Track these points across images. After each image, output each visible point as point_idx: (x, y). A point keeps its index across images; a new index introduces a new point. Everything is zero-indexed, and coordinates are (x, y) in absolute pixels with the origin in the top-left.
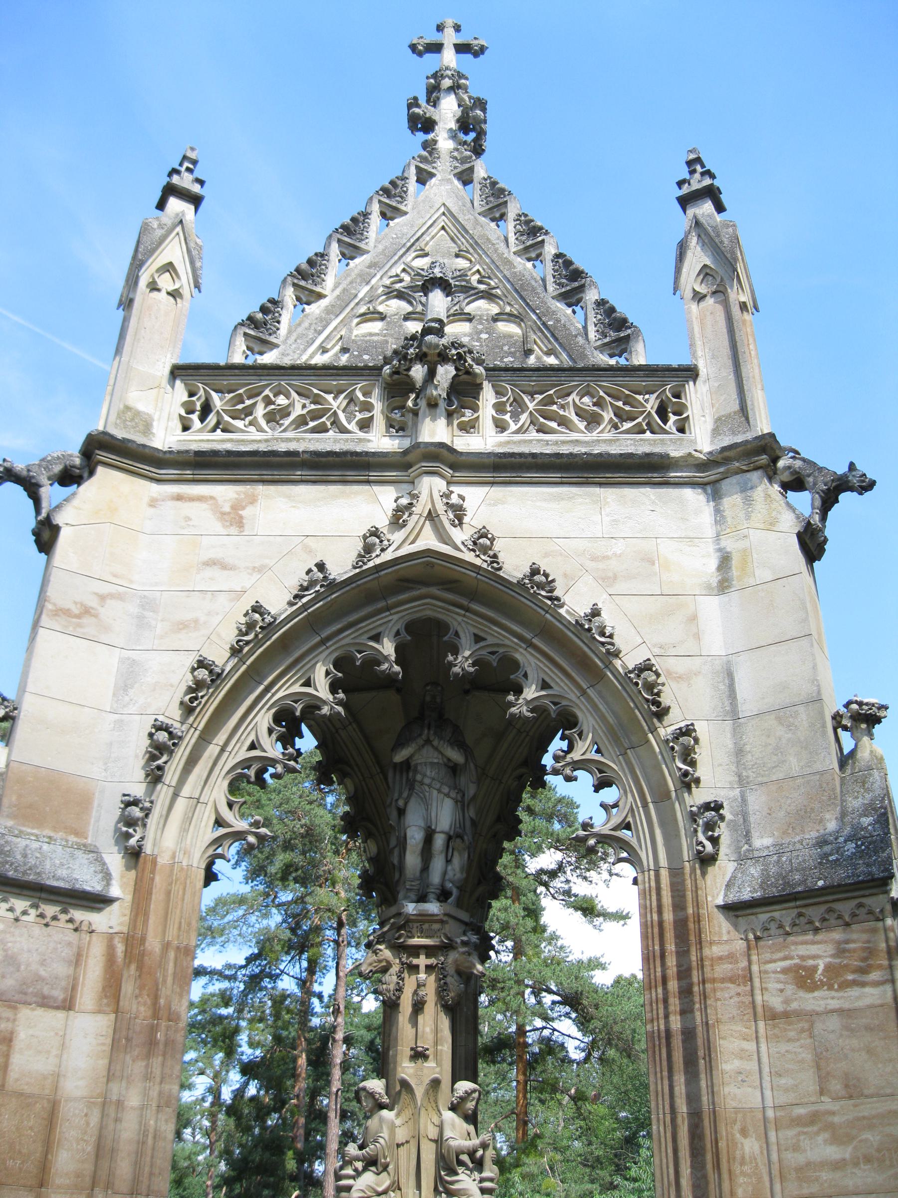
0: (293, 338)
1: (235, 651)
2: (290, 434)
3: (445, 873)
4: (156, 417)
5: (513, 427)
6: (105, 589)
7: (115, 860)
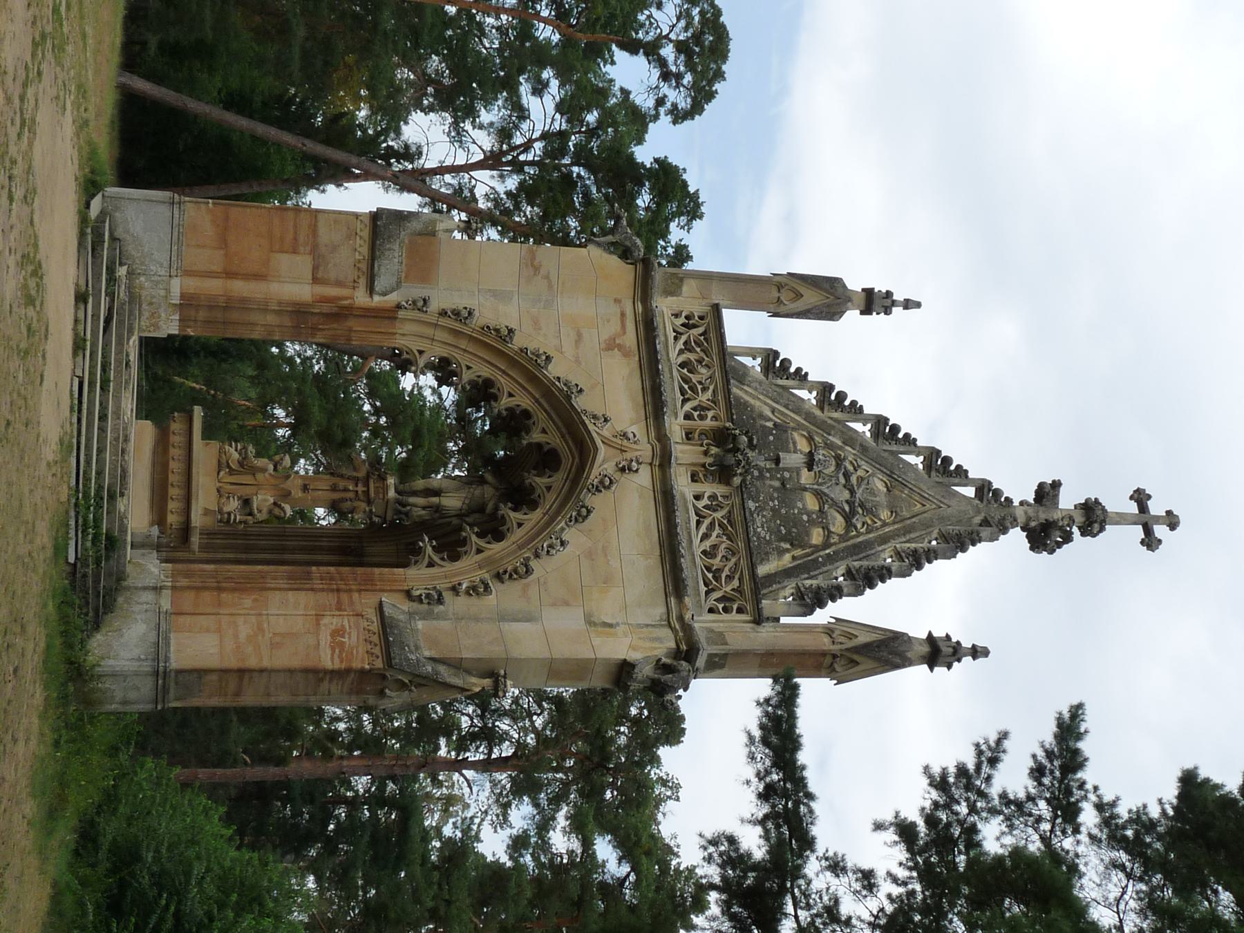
0: (777, 389)
1: (521, 350)
2: (675, 373)
3: (416, 506)
4: (680, 298)
5: (700, 505)
7: (393, 298)
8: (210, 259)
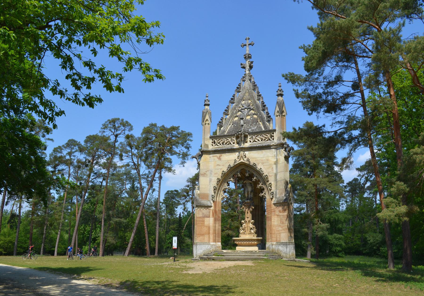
1: (221, 177)
5: (252, 141)
6: (207, 170)
7: (212, 202)
8: (206, 238)
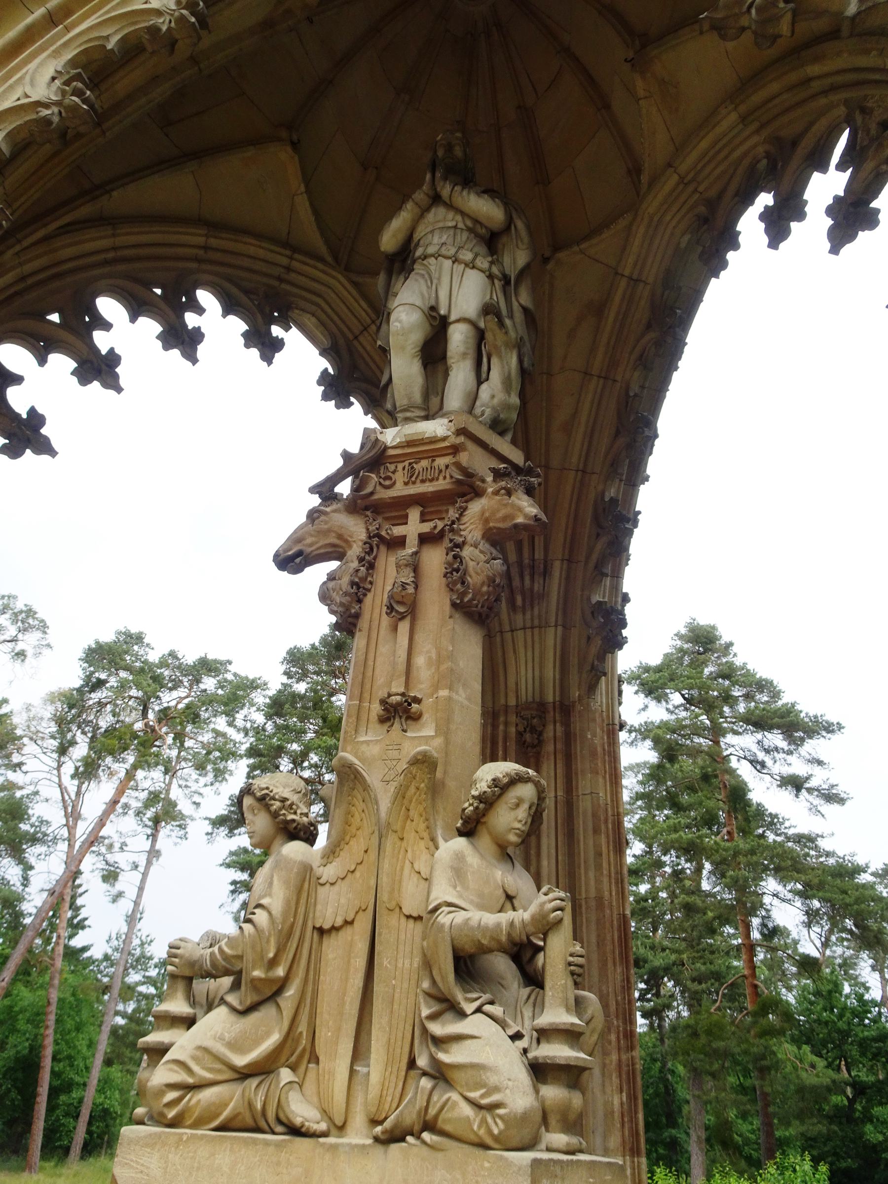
3: (474, 398)
